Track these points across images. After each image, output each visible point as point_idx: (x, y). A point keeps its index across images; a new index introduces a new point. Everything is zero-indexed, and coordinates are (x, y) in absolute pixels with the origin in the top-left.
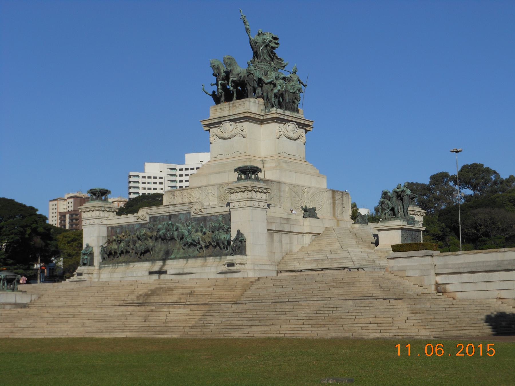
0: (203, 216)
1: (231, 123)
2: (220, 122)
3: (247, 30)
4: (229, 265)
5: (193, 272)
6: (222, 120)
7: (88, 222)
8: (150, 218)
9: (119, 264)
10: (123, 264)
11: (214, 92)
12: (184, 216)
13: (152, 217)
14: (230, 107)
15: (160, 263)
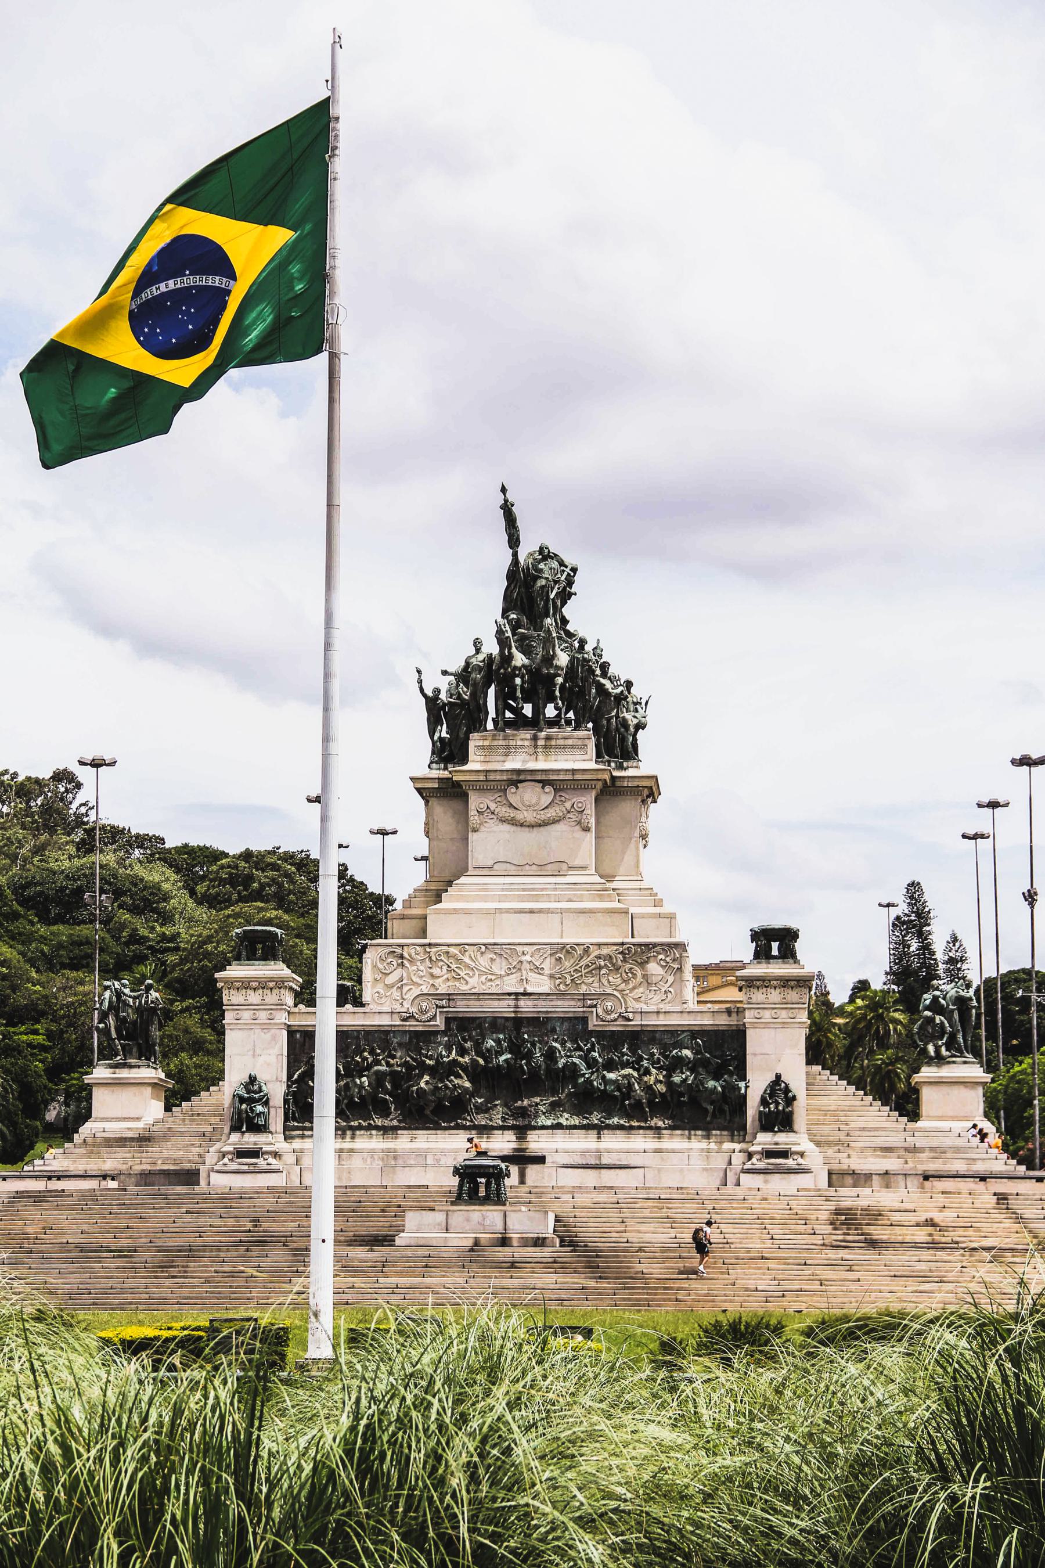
0: (630, 1029)
1: (548, 789)
2: (515, 783)
3: (514, 541)
4: (769, 1154)
5: (633, 1164)
6: (522, 778)
7: (246, 1015)
8: (448, 1021)
9: (358, 1132)
10: (374, 1132)
11: (437, 691)
12: (566, 1025)
13: (455, 1019)
14: (536, 746)
15: (510, 1136)
